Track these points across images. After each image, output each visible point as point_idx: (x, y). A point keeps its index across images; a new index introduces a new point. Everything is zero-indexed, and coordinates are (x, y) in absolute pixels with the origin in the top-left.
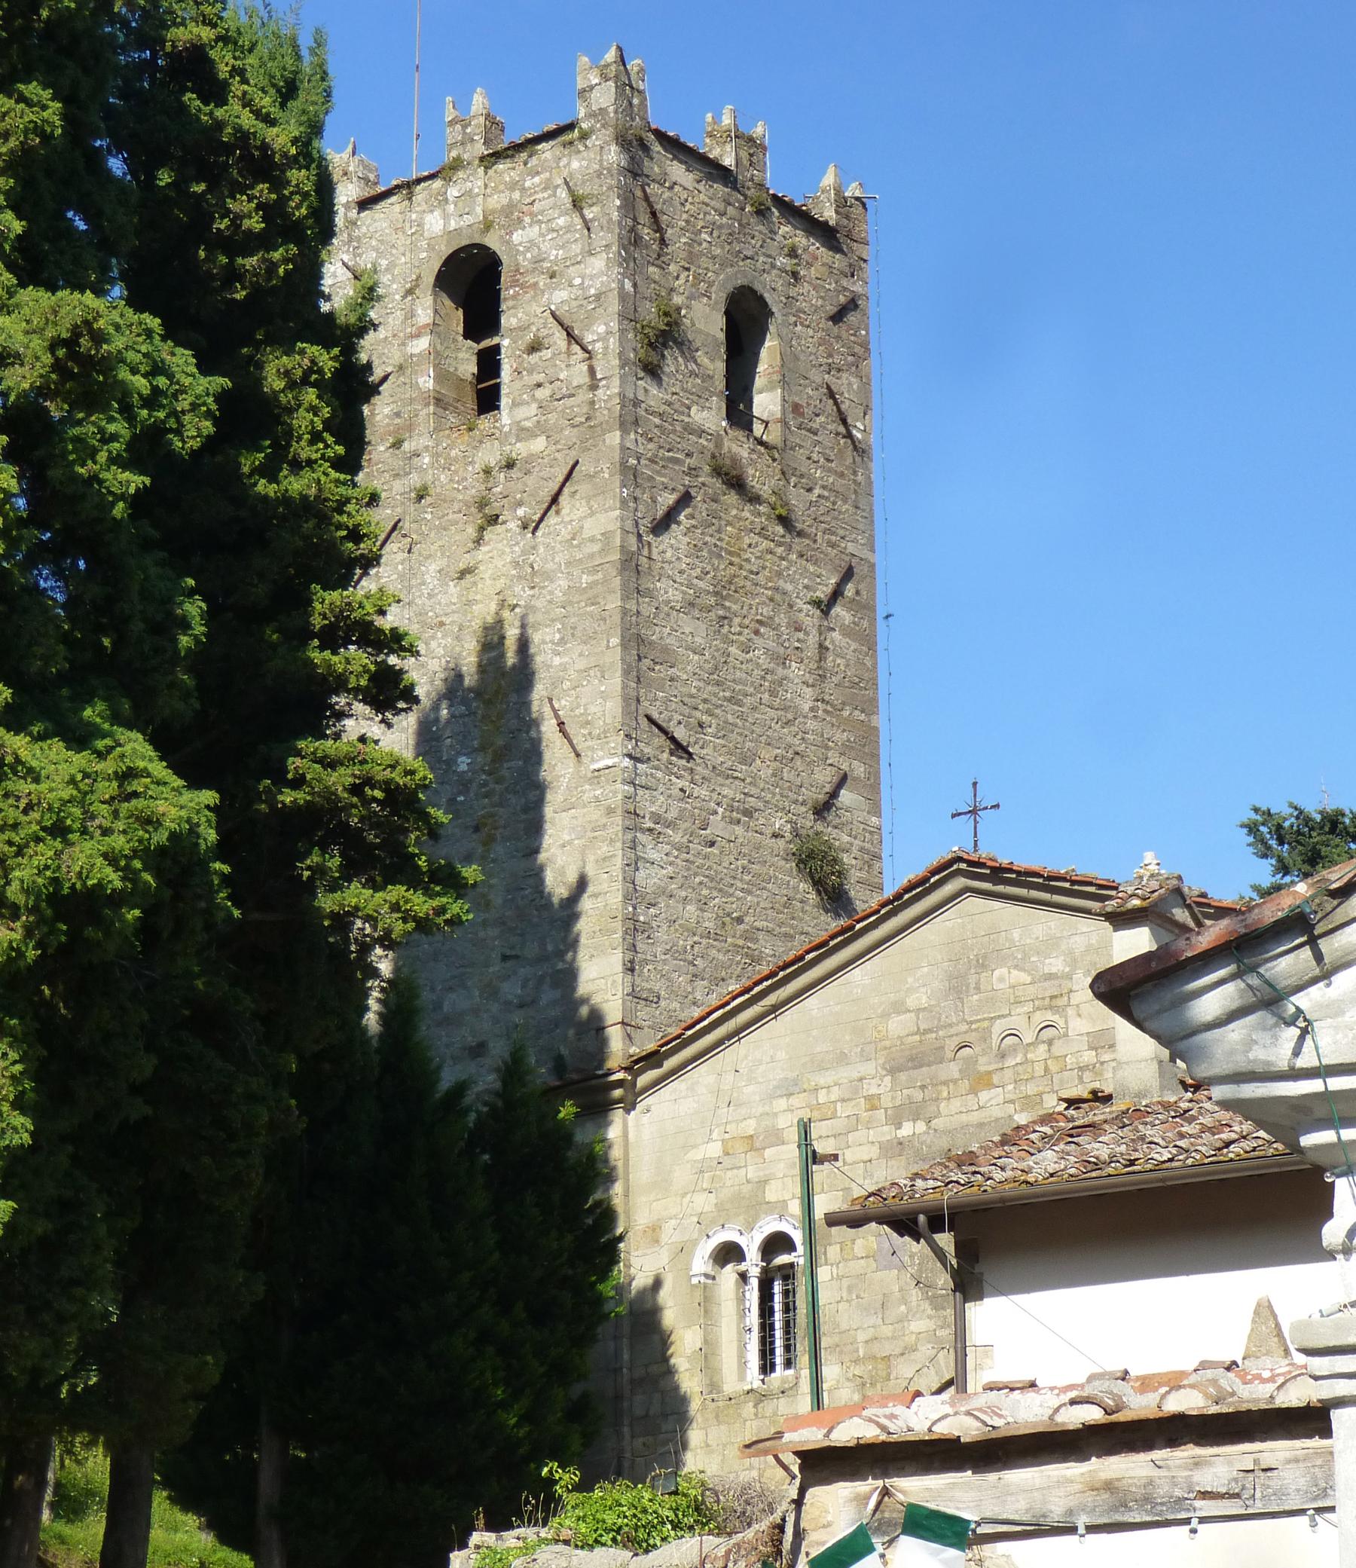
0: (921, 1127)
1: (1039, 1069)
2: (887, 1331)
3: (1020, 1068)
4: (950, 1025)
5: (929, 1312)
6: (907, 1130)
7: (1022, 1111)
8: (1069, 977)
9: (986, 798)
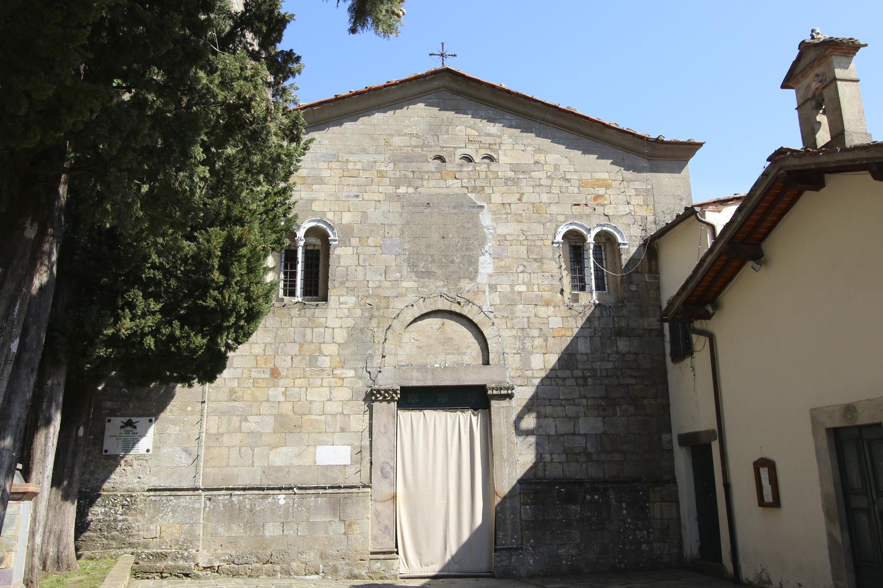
0: (411, 190)
1: (483, 175)
2: (388, 284)
3: (471, 173)
4: (431, 147)
5: (414, 278)
6: (402, 190)
7: (472, 192)
8: (500, 137)
9: (448, 51)
